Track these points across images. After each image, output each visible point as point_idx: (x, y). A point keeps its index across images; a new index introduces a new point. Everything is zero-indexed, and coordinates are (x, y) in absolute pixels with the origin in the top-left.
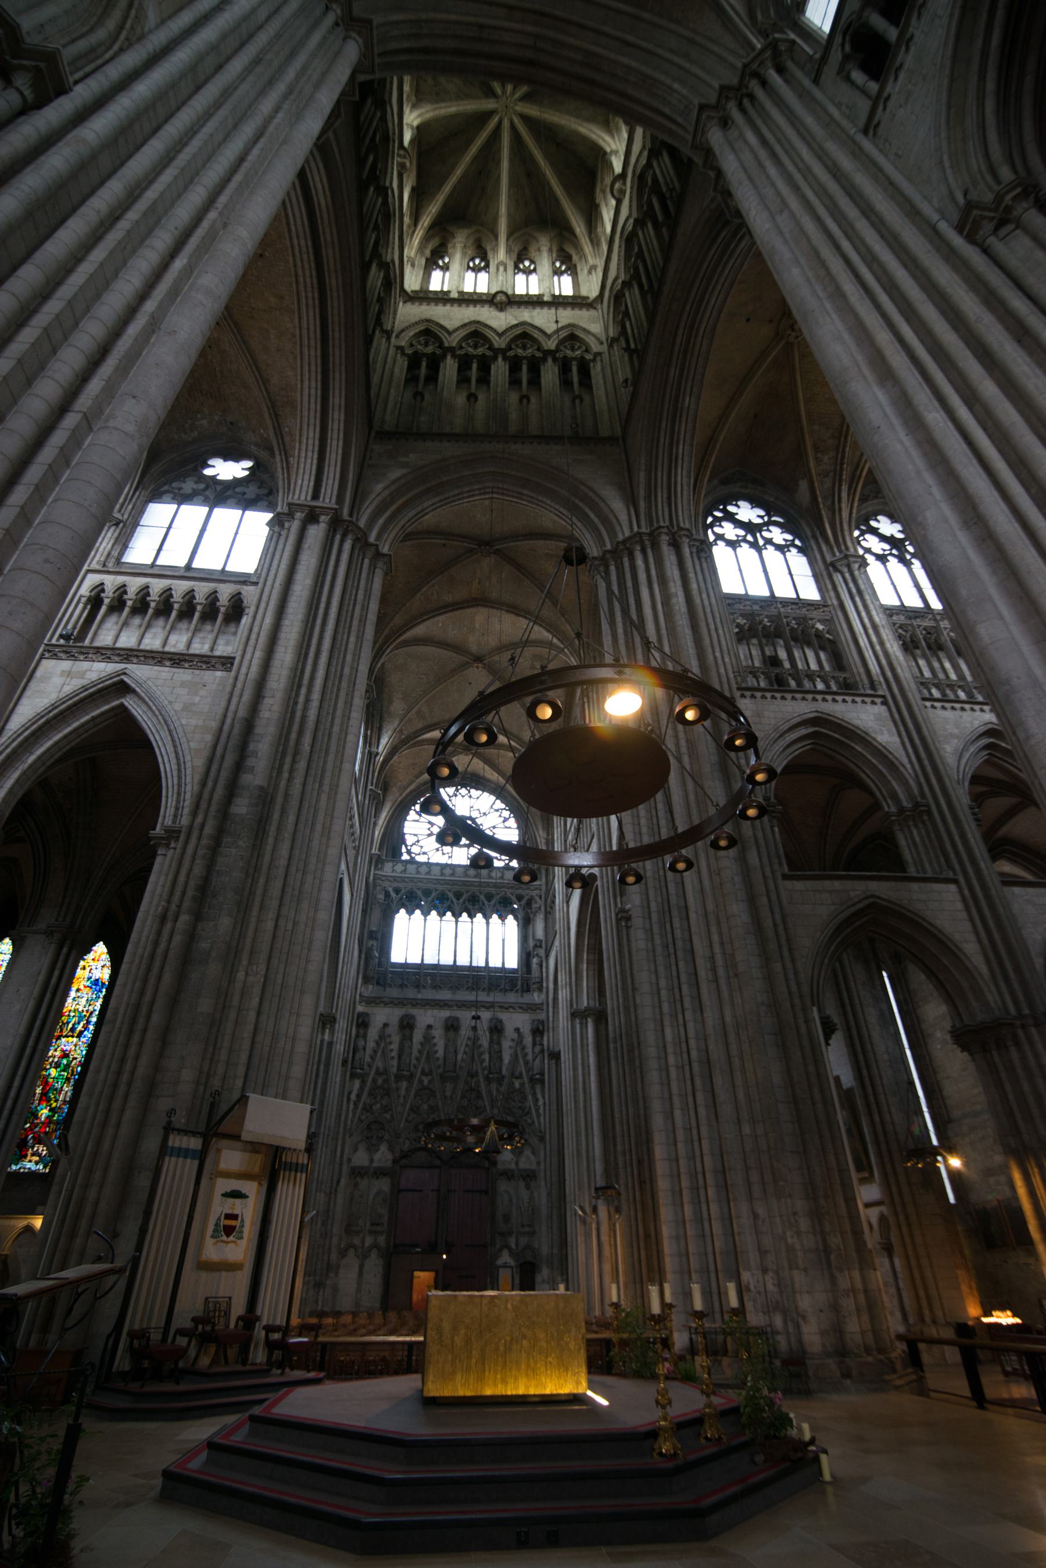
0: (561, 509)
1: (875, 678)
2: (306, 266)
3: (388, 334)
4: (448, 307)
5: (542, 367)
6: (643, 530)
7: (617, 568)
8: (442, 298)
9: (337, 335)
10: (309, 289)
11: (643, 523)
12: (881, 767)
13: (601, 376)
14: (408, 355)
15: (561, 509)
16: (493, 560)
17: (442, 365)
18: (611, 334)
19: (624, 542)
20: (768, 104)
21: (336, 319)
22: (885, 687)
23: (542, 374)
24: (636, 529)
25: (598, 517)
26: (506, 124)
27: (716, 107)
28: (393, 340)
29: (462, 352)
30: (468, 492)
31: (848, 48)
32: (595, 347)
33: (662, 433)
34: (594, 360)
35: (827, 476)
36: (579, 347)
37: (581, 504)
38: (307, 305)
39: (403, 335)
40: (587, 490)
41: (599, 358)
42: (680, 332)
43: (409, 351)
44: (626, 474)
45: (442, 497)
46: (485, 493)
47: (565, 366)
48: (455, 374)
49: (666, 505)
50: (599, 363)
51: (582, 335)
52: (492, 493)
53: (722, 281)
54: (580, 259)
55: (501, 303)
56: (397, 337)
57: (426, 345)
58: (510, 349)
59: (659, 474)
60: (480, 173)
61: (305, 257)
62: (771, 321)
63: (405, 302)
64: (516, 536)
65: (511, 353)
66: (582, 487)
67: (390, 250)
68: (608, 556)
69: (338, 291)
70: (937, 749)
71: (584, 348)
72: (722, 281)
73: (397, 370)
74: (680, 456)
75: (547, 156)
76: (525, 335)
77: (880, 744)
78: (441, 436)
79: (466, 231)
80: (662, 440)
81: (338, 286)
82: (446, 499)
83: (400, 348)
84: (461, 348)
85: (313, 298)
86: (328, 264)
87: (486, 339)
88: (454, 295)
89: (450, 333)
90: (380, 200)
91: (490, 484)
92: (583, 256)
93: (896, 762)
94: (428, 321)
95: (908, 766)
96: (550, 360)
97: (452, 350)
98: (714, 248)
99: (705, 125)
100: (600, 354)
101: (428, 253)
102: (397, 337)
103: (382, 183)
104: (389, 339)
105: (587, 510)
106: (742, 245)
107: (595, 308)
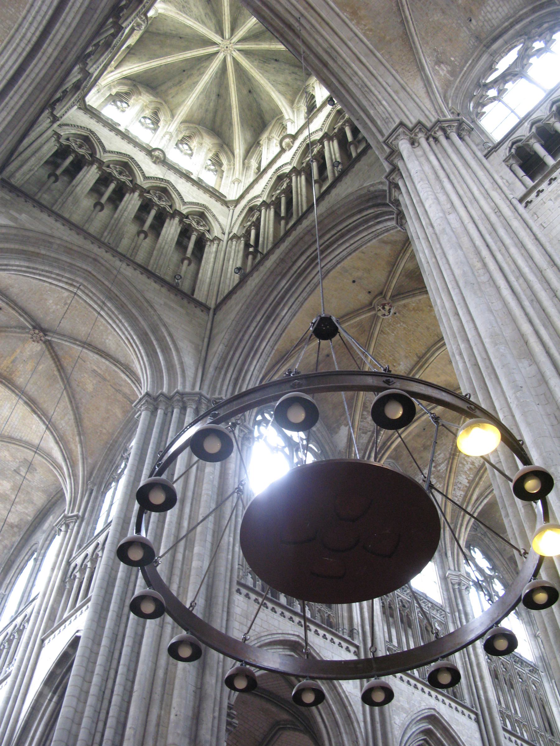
0: (135, 337)
1: (355, 627)
2: (35, 24)
3: (55, 119)
4: (113, 134)
5: (168, 221)
6: (204, 393)
7: (165, 414)
8: (113, 127)
9: (25, 86)
10: (25, 41)
11: (206, 387)
12: (337, 716)
13: (213, 255)
14: (61, 144)
15: (135, 337)
16: (39, 348)
17: (85, 168)
18: (235, 231)
19: (182, 395)
20: (450, 150)
21: (33, 75)
22: (361, 638)
23: (166, 225)
24: (197, 389)
26: (221, 56)
27: (411, 130)
28: (55, 125)
29: (109, 170)
30: (58, 275)
31: (513, 151)
32: (217, 232)
33: (254, 324)
34: (212, 241)
35: (365, 433)
36: (204, 226)
37: (155, 343)
38: (15, 50)
39: (66, 128)
40: (166, 334)
41: (216, 242)
42: (303, 258)
43: (65, 143)
44: (206, 340)
45: (31, 265)
46: (71, 285)
47: (185, 232)
48: (94, 181)
49: (232, 384)
50: (215, 246)
51: (210, 218)
52: (78, 288)
53: (352, 242)
54: (229, 169)
55: (157, 158)
56: (60, 126)
57: (80, 147)
58: (148, 192)
59: (237, 355)
60: (184, 71)
61: (39, 18)
62: (369, 292)
63: (79, 108)
64: (74, 339)
65: (148, 196)
66: (163, 330)
67: (95, 66)
68: (161, 398)
69: (49, 58)
70: (390, 716)
71: (208, 228)
72: (352, 242)
73: (46, 148)
74: (261, 351)
75: (239, 91)
76: (164, 191)
77: (344, 692)
78: (59, 217)
79: (152, 98)
80: (252, 329)
81: (51, 55)
82: (33, 268)
83: (56, 133)
84: (108, 166)
85: (24, 49)
86: (55, 36)
87: (131, 173)
88: (122, 128)
89: (105, 151)
90: (112, 31)
91: (81, 281)
92: (232, 167)
93: (352, 715)
94: (91, 131)
95: (362, 724)
96: (177, 220)
97: (101, 163)
98: (359, 216)
99: (399, 135)
100: (219, 240)
101: (114, 92)
102: (60, 126)
103: (120, 22)
104: (53, 122)
105: (158, 351)
106: (378, 227)
107: (228, 207)
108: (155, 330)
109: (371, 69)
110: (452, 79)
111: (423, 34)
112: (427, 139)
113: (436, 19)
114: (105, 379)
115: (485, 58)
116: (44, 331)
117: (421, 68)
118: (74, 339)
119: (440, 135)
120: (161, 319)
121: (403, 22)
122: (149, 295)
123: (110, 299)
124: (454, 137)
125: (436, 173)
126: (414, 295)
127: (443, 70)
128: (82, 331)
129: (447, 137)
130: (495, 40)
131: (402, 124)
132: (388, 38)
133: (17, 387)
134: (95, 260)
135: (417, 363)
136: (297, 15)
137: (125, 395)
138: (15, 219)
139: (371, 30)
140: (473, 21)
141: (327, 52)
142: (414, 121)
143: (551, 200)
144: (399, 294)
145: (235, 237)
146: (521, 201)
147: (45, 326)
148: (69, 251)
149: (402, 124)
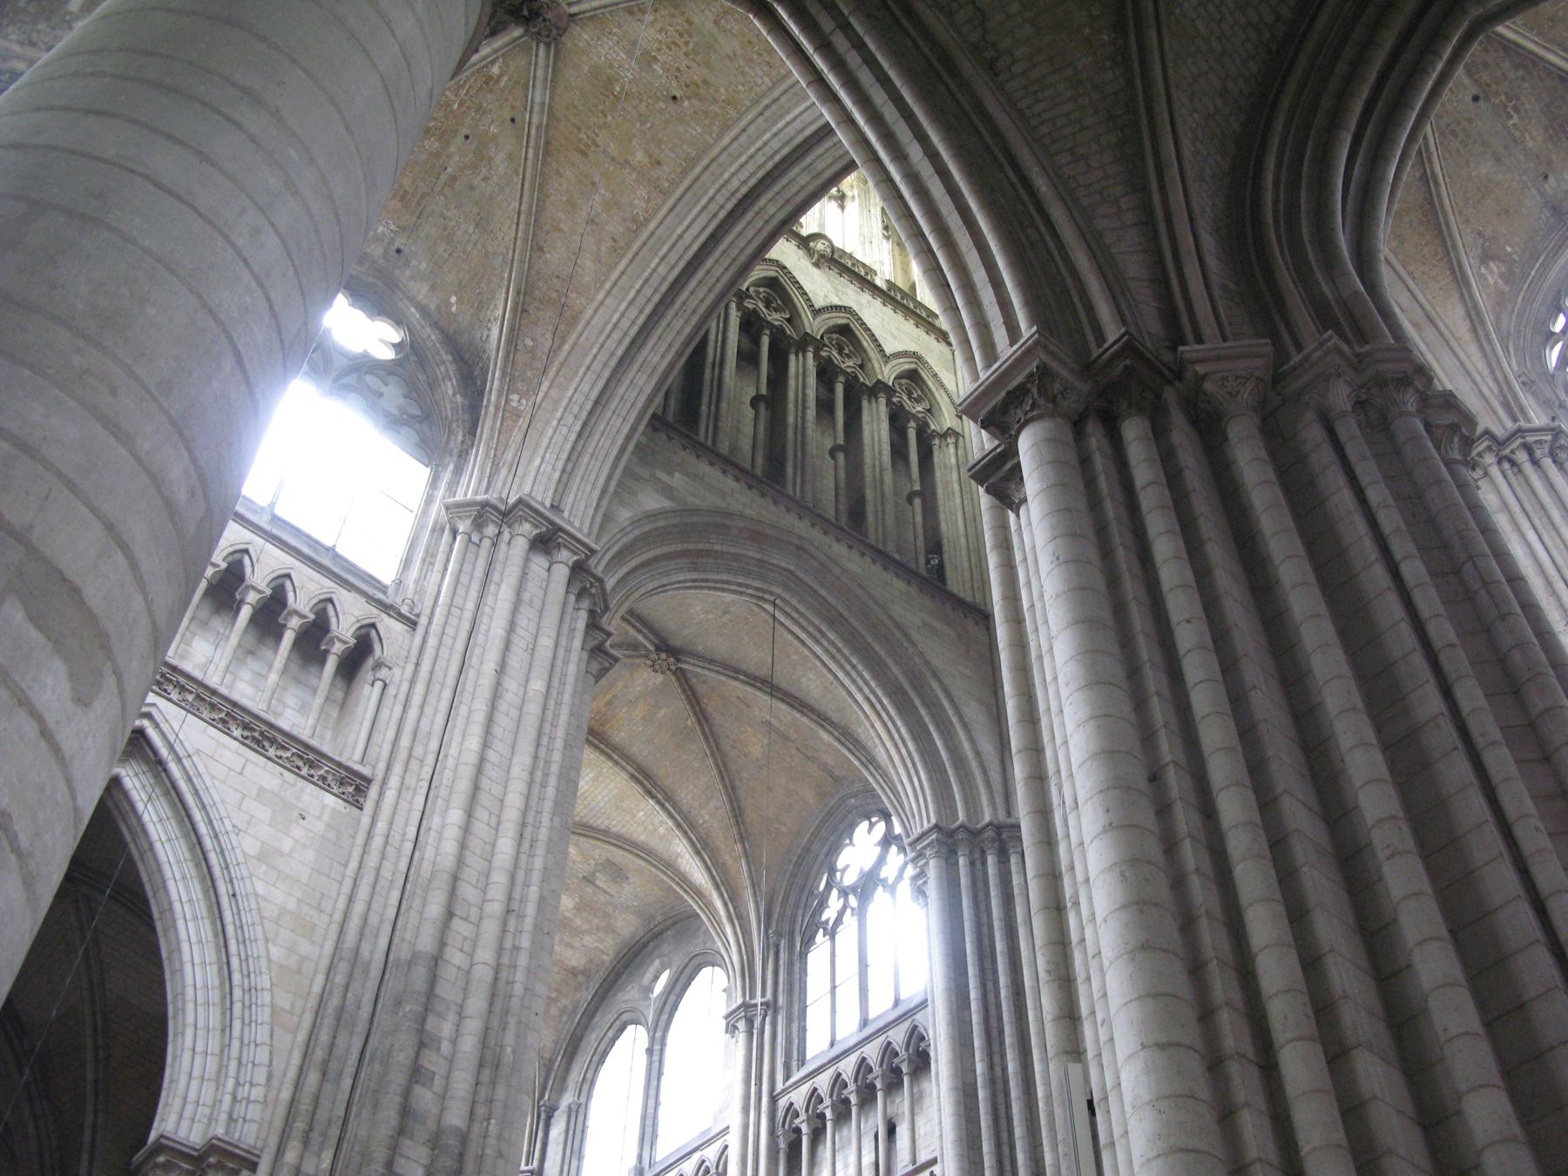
0: (885, 702)
7: (972, 863)
10: (726, 193)
15: (885, 702)
25: (946, 744)
30: (740, 585)
41: (951, 440)
64: (734, 671)
66: (935, 686)
69: (767, 222)
87: (788, 303)
105: (932, 728)
108: (918, 685)
110: (1507, 289)
111: (1461, 203)
112: (1499, 463)
113: (1484, 171)
114: (786, 738)
116: (674, 652)
117: (1461, 282)
118: (734, 671)
119: (1522, 457)
120: (927, 662)
122: (898, 610)
123: (830, 623)
124: (1547, 462)
127: (1492, 272)
128: (755, 658)
129: (1535, 463)
133: (615, 749)
134: (800, 548)
137: (824, 767)
138: (667, 491)
140: (1551, 180)
147: (676, 642)
148: (756, 536)
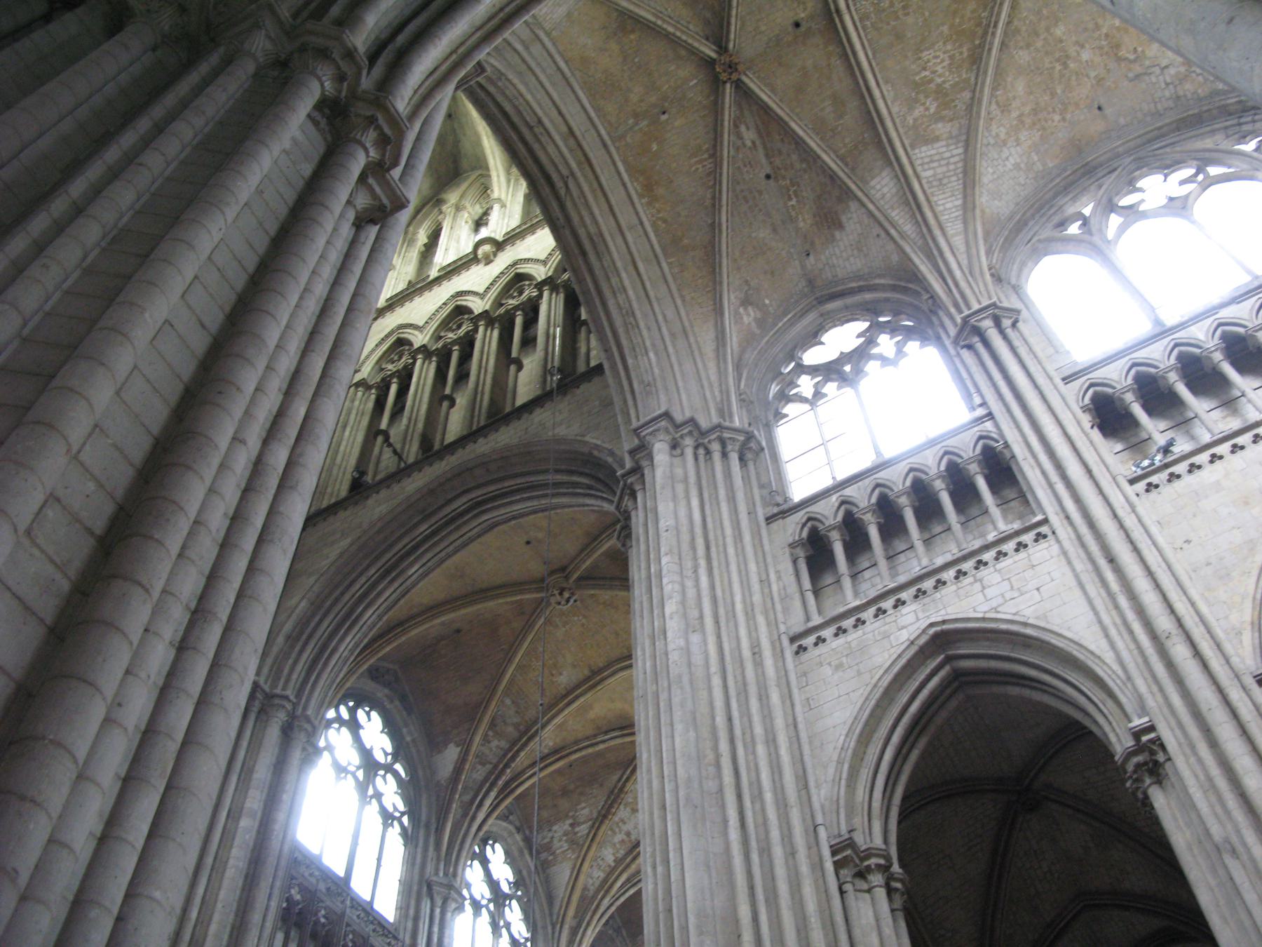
27: (677, 427)
33: (363, 579)
42: (464, 499)
80: (357, 586)
99: (658, 430)
109: (648, 285)
110: (757, 331)
111: (737, 254)
112: (696, 448)
113: (762, 235)
115: (811, 317)
117: (718, 311)
121: (714, 227)
124: (734, 457)
125: (693, 539)
126: (611, 588)
127: (749, 315)
129: (724, 455)
130: (833, 297)
131: (667, 415)
132: (686, 241)
135: (588, 679)
136: (565, 172)
139: (665, 221)
140: (812, 258)
141: (591, 239)
142: (688, 414)
143: (829, 664)
144: (591, 579)
145: (362, 384)
146: (793, 640)
149: (667, 415)
